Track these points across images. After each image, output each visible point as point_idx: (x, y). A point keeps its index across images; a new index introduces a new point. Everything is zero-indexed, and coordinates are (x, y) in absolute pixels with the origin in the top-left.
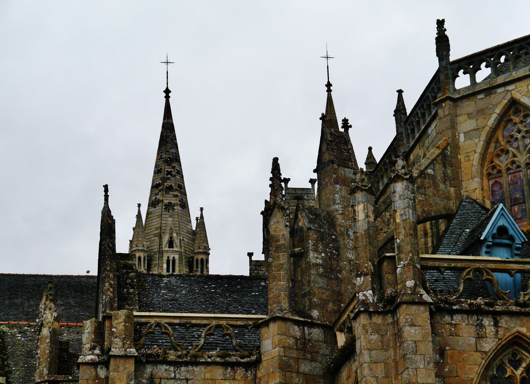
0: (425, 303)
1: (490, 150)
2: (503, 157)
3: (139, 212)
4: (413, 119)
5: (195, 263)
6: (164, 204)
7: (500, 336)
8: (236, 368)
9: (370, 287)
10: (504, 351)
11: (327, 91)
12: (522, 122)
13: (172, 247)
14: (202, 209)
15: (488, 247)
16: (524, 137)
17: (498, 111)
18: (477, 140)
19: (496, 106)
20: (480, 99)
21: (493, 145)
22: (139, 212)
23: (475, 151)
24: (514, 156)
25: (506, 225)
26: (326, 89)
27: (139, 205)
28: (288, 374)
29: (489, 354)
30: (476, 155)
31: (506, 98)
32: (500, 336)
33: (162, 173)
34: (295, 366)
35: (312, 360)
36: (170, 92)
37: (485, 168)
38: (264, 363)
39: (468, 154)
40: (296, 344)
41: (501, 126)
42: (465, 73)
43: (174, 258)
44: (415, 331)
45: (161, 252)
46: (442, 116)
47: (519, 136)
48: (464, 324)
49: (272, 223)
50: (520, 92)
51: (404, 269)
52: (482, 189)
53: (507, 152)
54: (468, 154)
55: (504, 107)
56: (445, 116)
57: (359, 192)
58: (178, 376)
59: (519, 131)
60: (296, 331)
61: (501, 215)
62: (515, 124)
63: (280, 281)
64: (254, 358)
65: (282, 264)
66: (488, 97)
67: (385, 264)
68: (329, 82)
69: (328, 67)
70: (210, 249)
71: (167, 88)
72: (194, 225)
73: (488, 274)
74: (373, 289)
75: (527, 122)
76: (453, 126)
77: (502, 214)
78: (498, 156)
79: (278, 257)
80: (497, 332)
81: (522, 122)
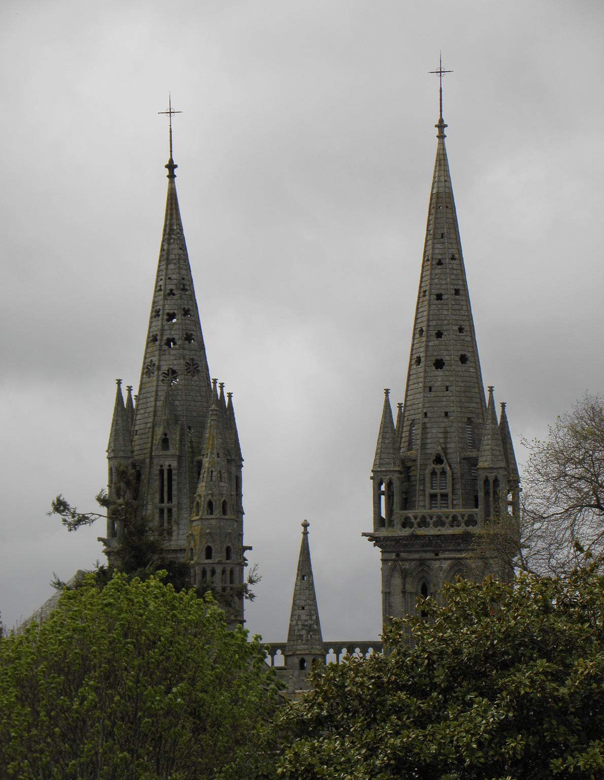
6: (161, 372)
36: (176, 166)
43: (170, 466)
69: (441, 91)
71: (171, 161)
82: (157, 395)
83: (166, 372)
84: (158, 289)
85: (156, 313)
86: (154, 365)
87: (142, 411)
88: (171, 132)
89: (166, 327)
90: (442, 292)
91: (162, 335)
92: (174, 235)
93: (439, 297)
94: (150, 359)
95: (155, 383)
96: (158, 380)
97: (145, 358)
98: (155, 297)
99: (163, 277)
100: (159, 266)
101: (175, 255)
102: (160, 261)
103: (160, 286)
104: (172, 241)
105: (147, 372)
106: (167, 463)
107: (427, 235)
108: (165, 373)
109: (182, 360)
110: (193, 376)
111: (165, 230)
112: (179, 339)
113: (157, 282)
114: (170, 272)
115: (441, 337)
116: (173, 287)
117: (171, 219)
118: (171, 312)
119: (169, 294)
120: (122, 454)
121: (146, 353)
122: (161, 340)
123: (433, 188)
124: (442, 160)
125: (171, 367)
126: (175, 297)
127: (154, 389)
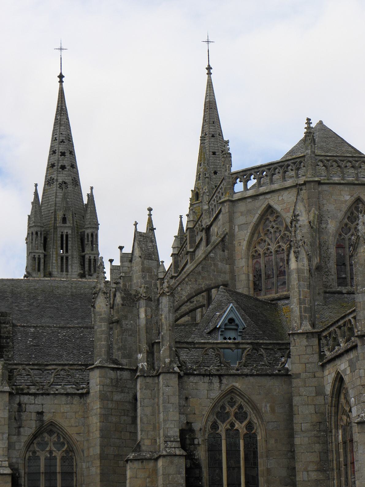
0: (175, 373)
1: (254, 239)
2: (263, 244)
3: (36, 190)
4: (213, 202)
5: (86, 237)
6: (58, 183)
7: (222, 389)
8: (74, 397)
9: (145, 360)
10: (225, 397)
11: (207, 74)
12: (275, 221)
13: (66, 223)
14: (92, 188)
15: (222, 331)
16: (275, 232)
17: (259, 212)
18: (246, 232)
19: (258, 208)
20: (249, 202)
21: (256, 235)
22: (36, 190)
23: (244, 239)
24: (269, 245)
25: (234, 317)
26: (207, 71)
27: (36, 185)
28: (106, 402)
29: (215, 400)
30: (245, 242)
31: (264, 203)
32: (222, 389)
33: (57, 154)
34: (110, 397)
35: (122, 392)
37: (251, 251)
38: (91, 394)
39: (240, 241)
40: (112, 382)
41: (262, 222)
42: (240, 181)
43: (67, 233)
44: (169, 390)
45: (55, 228)
46: (224, 213)
47: (272, 230)
48: (201, 382)
49: (98, 303)
50: (274, 201)
51: (165, 351)
52: (248, 267)
53: (265, 241)
54: (240, 241)
55: (263, 210)
56: (225, 213)
57: (142, 299)
58: (36, 402)
59: (273, 227)
60: (112, 374)
61: (231, 310)
62: (271, 221)
63: (102, 342)
64: (85, 391)
65: (104, 330)
66: (254, 201)
67: (155, 346)
68: (209, 65)
69: (208, 51)
70: (99, 224)
71: (61, 73)
72: (85, 201)
73: (218, 350)
74: (147, 362)
75: (278, 221)
76: (231, 220)
77: (232, 310)
78: (259, 243)
79: (101, 325)
80: (220, 387)
81: (275, 221)
82: (56, 195)
83: (61, 183)
84: (54, 139)
85: (53, 152)
86: (54, 179)
87: (46, 205)
88: (61, 59)
89: (60, 159)
90: (216, 151)
91: (58, 163)
92: (63, 111)
93: (214, 153)
94: (50, 177)
95: (55, 188)
96: (56, 187)
97: (46, 176)
98: (52, 143)
99: (57, 133)
100: (54, 128)
101: (64, 122)
102: (55, 125)
103: (56, 138)
104: (62, 114)
105: (48, 184)
106: (65, 231)
107: (203, 123)
108: (60, 183)
109: (70, 177)
110: (76, 187)
111: (57, 109)
112: (68, 166)
113: (53, 136)
114: (61, 130)
115: (216, 174)
116: (64, 138)
117: (61, 103)
118: (63, 151)
119: (61, 142)
120: (39, 224)
121: (47, 173)
122: (58, 166)
123: (206, 99)
124: (210, 85)
125: (64, 180)
126: (65, 144)
127: (55, 191)
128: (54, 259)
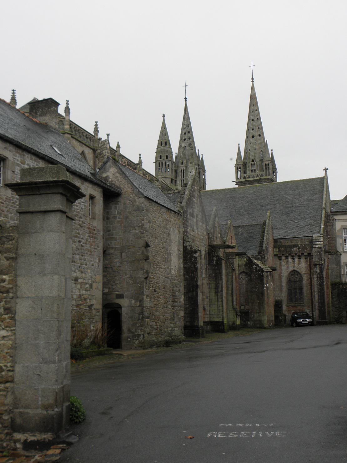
68: (252, 78)
90: (254, 119)
106: (183, 168)
128: (179, 181)
